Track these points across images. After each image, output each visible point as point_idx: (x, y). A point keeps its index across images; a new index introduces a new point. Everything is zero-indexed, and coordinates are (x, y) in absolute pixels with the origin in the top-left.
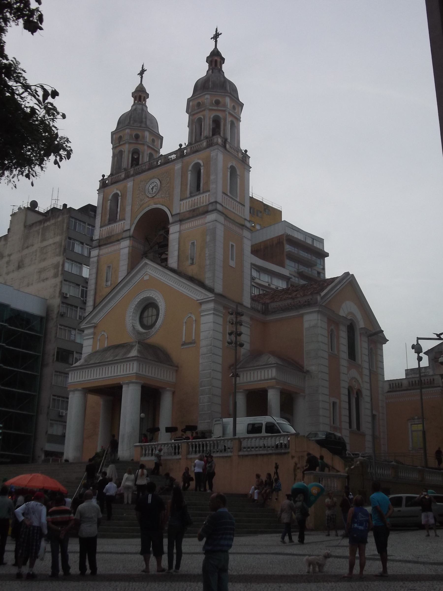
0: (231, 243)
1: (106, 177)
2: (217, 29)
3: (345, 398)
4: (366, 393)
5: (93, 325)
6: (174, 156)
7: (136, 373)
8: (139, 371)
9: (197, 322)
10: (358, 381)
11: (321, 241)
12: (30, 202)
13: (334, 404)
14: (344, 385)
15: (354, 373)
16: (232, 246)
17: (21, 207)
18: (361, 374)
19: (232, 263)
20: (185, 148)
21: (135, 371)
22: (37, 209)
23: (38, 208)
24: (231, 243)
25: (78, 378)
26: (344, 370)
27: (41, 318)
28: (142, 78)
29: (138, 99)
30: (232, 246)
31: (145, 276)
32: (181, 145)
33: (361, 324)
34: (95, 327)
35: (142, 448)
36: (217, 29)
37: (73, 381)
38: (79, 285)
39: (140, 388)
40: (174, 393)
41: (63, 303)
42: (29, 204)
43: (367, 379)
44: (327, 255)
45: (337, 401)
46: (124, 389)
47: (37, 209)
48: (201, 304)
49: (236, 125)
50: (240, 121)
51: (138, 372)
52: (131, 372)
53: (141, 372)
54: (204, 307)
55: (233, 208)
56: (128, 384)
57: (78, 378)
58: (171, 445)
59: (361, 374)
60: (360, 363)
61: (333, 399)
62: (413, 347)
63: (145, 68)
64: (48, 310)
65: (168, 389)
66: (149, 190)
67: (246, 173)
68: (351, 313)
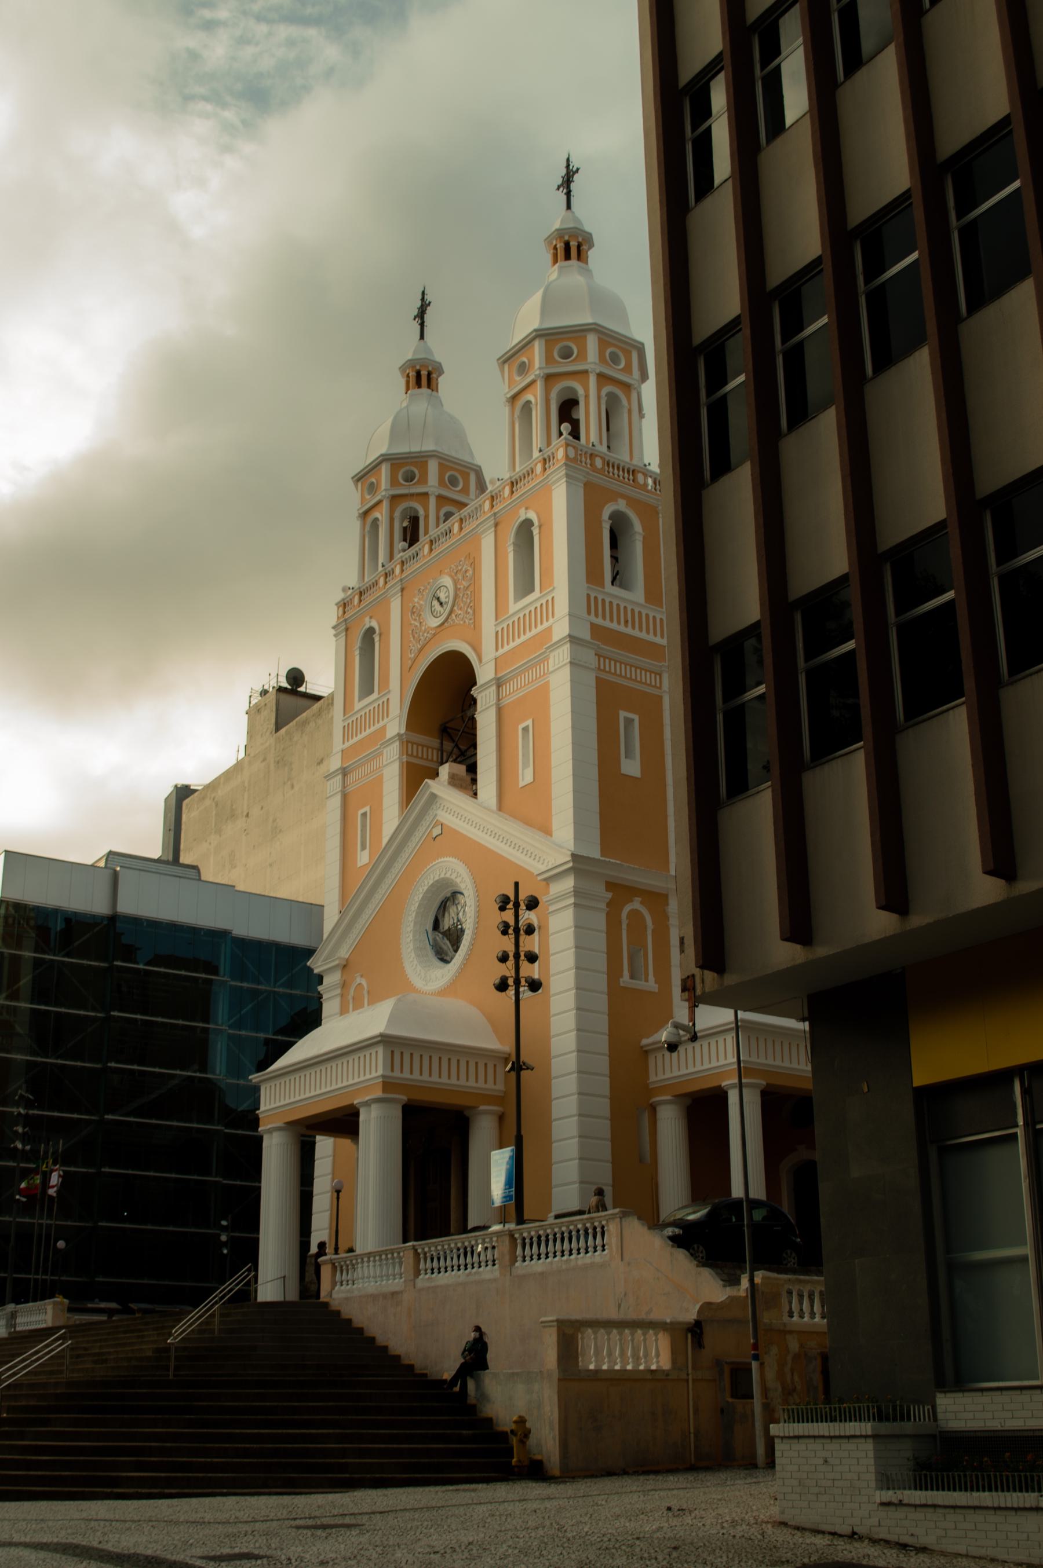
0: (623, 714)
5: (337, 962)
7: (383, 1076)
8: (392, 1070)
16: (629, 722)
17: (266, 687)
19: (632, 767)
21: (380, 1072)
22: (302, 689)
23: (304, 685)
24: (623, 714)
25: (268, 1103)
30: (629, 722)
31: (434, 830)
34: (345, 967)
35: (334, 1268)
47: (302, 689)
51: (389, 1074)
53: (397, 1074)
55: (626, 622)
57: (268, 1103)
58: (381, 1256)
65: (482, 1108)
66: (433, 609)
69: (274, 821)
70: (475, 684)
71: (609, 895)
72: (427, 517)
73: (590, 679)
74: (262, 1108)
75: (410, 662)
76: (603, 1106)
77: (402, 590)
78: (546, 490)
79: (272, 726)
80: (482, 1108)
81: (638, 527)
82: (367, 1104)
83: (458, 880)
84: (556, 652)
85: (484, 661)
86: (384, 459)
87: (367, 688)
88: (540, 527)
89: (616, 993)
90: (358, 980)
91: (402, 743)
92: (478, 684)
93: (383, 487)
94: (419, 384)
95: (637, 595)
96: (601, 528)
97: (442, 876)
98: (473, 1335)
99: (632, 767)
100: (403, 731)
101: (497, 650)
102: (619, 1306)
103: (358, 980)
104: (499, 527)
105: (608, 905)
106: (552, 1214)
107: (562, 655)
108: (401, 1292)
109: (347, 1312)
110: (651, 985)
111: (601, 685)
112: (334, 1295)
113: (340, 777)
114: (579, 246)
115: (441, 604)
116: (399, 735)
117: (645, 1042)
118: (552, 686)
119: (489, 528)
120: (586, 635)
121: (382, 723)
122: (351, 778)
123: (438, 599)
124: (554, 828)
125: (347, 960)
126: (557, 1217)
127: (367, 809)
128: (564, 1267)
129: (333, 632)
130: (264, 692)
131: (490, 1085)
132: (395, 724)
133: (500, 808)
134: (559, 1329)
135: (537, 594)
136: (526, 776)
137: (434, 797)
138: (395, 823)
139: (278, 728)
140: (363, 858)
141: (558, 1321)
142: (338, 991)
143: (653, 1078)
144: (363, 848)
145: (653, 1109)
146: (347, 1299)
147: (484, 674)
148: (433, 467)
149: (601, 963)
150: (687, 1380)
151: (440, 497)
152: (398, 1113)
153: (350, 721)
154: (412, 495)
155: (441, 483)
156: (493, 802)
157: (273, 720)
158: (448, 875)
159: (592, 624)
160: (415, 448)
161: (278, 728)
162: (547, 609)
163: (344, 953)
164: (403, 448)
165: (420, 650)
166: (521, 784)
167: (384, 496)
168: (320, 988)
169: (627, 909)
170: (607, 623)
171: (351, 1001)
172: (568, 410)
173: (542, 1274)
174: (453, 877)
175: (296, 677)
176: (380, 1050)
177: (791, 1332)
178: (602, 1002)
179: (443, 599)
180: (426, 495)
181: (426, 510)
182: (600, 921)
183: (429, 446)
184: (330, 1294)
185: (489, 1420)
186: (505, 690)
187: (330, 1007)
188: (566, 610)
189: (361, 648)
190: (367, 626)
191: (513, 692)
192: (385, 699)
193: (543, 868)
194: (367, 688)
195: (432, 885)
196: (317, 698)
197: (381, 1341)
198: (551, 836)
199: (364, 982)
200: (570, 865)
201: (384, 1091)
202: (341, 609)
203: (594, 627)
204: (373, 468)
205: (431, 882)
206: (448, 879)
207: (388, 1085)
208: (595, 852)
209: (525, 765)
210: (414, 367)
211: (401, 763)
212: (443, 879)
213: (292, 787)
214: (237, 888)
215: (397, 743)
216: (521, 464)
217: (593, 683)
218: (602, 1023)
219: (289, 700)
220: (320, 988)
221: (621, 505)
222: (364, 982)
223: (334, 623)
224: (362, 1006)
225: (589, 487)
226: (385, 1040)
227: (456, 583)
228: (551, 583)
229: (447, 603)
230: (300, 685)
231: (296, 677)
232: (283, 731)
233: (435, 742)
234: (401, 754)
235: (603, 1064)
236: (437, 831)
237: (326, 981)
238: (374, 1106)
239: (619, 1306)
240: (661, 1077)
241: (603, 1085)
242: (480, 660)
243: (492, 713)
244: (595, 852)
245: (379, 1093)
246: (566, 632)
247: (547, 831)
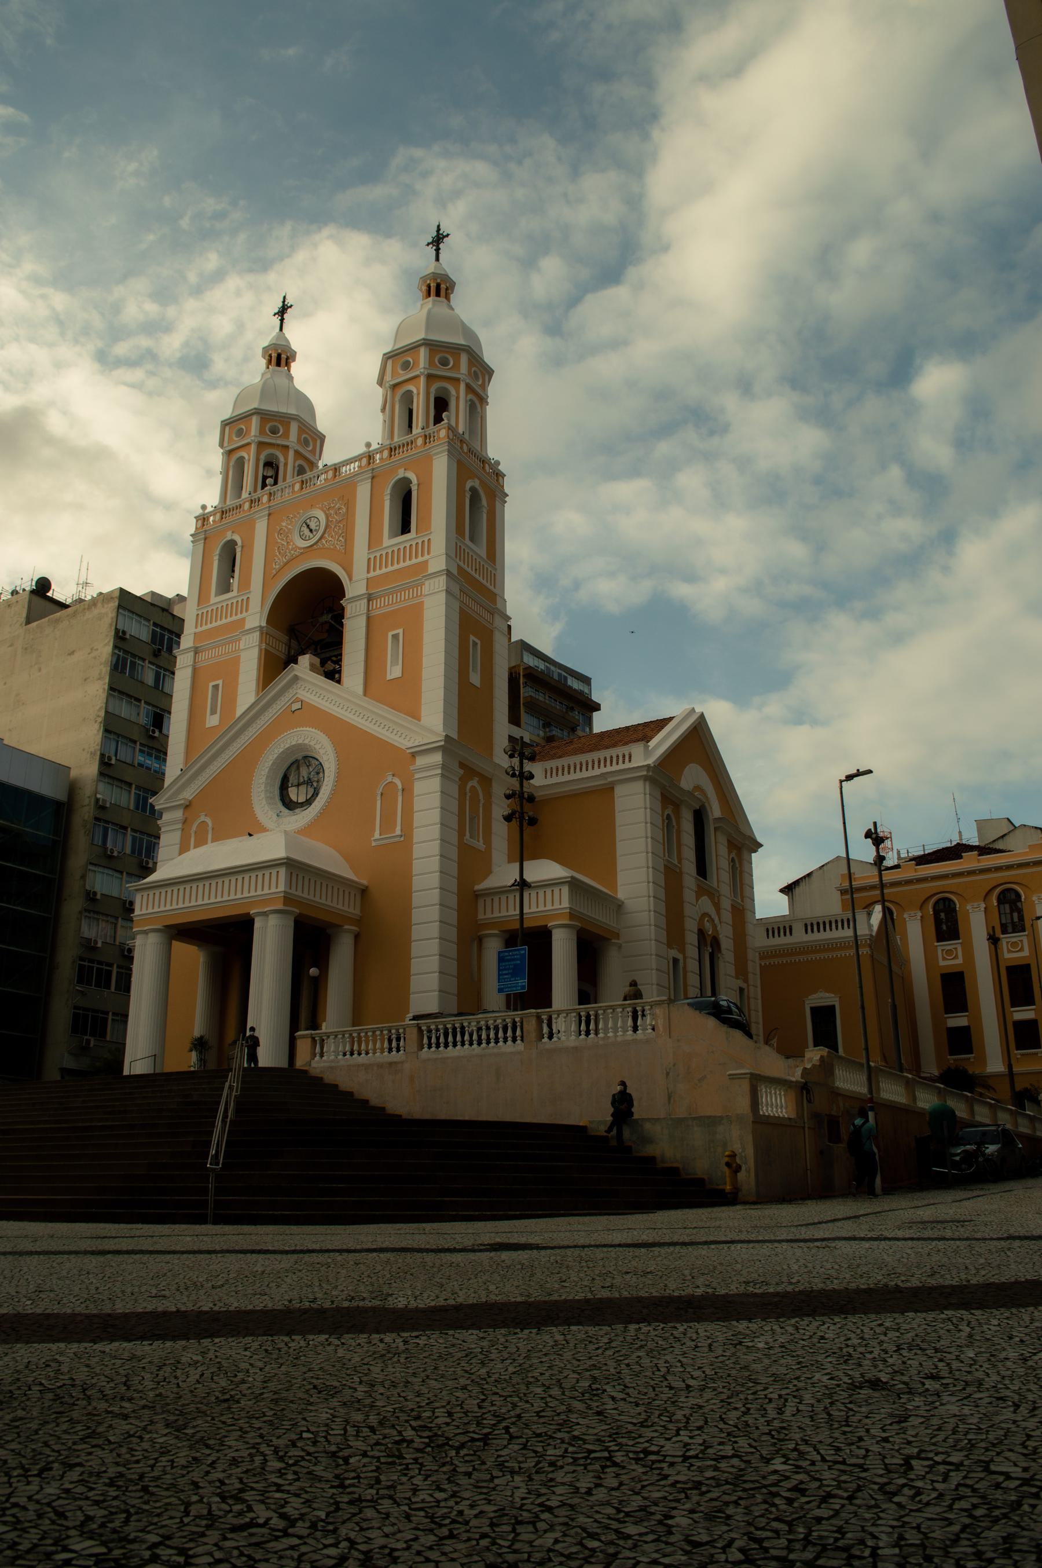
0: (472, 638)
1: (209, 509)
2: (439, 226)
3: (692, 951)
4: (727, 944)
6: (354, 467)
7: (285, 892)
9: (407, 791)
10: (713, 921)
11: (586, 680)
12: (35, 579)
13: (675, 961)
14: (691, 926)
15: (706, 904)
16: (475, 644)
18: (717, 906)
20: (377, 451)
22: (49, 594)
24: (472, 638)
26: (689, 895)
27: (58, 804)
28: (282, 320)
29: (274, 360)
30: (475, 644)
32: (368, 445)
33: (715, 811)
34: (187, 807)
36: (439, 226)
37: (144, 912)
38: (135, 742)
39: (292, 924)
40: (357, 937)
41: (101, 774)
42: (34, 583)
43: (727, 916)
44: (597, 707)
45: (680, 956)
46: (258, 924)
47: (49, 594)
48: (414, 755)
49: (479, 409)
50: (487, 404)
51: (288, 890)
52: (273, 890)
53: (293, 891)
54: (421, 761)
56: (265, 914)
58: (382, 1031)
59: (717, 906)
60: (715, 885)
61: (674, 953)
62: (868, 835)
63: (289, 302)
64: (73, 788)
65: (346, 927)
67: (498, 505)
68: (698, 788)
69: (17, 695)
70: (344, 596)
71: (462, 772)
72: (286, 464)
73: (456, 605)
74: (137, 912)
75: (274, 572)
76: (453, 934)
77: (269, 515)
78: (428, 460)
79: (23, 619)
80: (346, 927)
81: (484, 502)
82: (265, 914)
83: (317, 747)
84: (432, 581)
85: (354, 579)
86: (257, 412)
87: (225, 587)
88: (419, 485)
89: (464, 849)
90: (203, 818)
91: (262, 634)
92: (347, 597)
93: (253, 433)
94: (278, 364)
95: (483, 552)
96: (465, 496)
97: (300, 741)
98: (619, 1088)
99: (475, 679)
100: (264, 624)
101: (368, 572)
102: (668, 1074)
103: (203, 818)
104: (375, 480)
105: (460, 779)
106: (410, 1015)
107: (441, 582)
108: (402, 1063)
109: (329, 1078)
110: (481, 845)
111: (462, 613)
112: (314, 1064)
113: (192, 654)
114: (447, 289)
115: (311, 531)
116: (261, 627)
117: (477, 887)
118: (426, 606)
119: (366, 479)
120: (455, 572)
121: (244, 614)
122: (202, 656)
123: (308, 526)
124: (423, 714)
125: (190, 802)
126: (415, 1018)
127: (220, 682)
128: (601, 1042)
129: (191, 539)
130: (14, 593)
131: (351, 910)
132: (256, 616)
133: (365, 694)
134: (750, 1079)
135: (412, 534)
136: (394, 672)
137: (296, 678)
138: (251, 698)
139: (28, 622)
140: (213, 721)
141: (752, 1074)
142: (180, 826)
143: (481, 916)
144: (213, 712)
145: (480, 940)
146: (331, 1068)
147: (354, 588)
148: (294, 428)
149: (454, 822)
150: (804, 1128)
151: (297, 452)
152: (291, 923)
153: (205, 611)
154: (278, 445)
155: (299, 440)
156: (360, 690)
157: (24, 615)
158: (306, 742)
159: (459, 567)
160: (283, 409)
161: (28, 622)
162: (426, 547)
163: (188, 794)
164: (273, 408)
165: (286, 564)
166: (389, 677)
167: (253, 441)
168: (159, 822)
169: (470, 784)
170: (465, 567)
171: (193, 835)
172: (441, 405)
173: (575, 1048)
174: (312, 743)
175: (43, 586)
176: (283, 871)
177: (840, 1095)
178: (454, 853)
179: (313, 526)
180: (287, 447)
181: (286, 459)
182: (454, 790)
183: (292, 411)
184: (309, 1064)
185: (652, 1159)
186: (374, 604)
187: (169, 840)
188: (443, 550)
189: (220, 555)
190: (229, 538)
191: (381, 607)
192: (245, 598)
193: (410, 745)
194: (225, 587)
195: (288, 749)
196: (63, 606)
197: (375, 1101)
198: (419, 720)
199: (209, 821)
200: (442, 743)
201: (285, 904)
202: (200, 522)
203: (460, 569)
204: (246, 417)
205: (287, 746)
206: (305, 745)
207: (288, 899)
208: (455, 736)
209: (395, 662)
210: (276, 350)
211: (260, 650)
212: (300, 745)
213: (40, 670)
214: (5, 742)
215: (258, 633)
216: (399, 436)
217: (458, 610)
218: (454, 869)
219: (37, 599)
220: (159, 822)
221: (476, 483)
222: (209, 821)
223: (193, 532)
224: (205, 843)
225: (460, 464)
226: (291, 865)
227: (327, 517)
228: (429, 527)
229: (317, 531)
230: (48, 591)
231: (43, 586)
232: (34, 624)
233: (285, 638)
234: (261, 642)
235: (453, 901)
236: (297, 706)
237: (166, 817)
238: (271, 916)
239: (668, 1074)
240: (489, 915)
241: (453, 917)
242: (350, 579)
243: (362, 621)
244: (455, 736)
245: (280, 906)
246: (444, 567)
247: (415, 715)
